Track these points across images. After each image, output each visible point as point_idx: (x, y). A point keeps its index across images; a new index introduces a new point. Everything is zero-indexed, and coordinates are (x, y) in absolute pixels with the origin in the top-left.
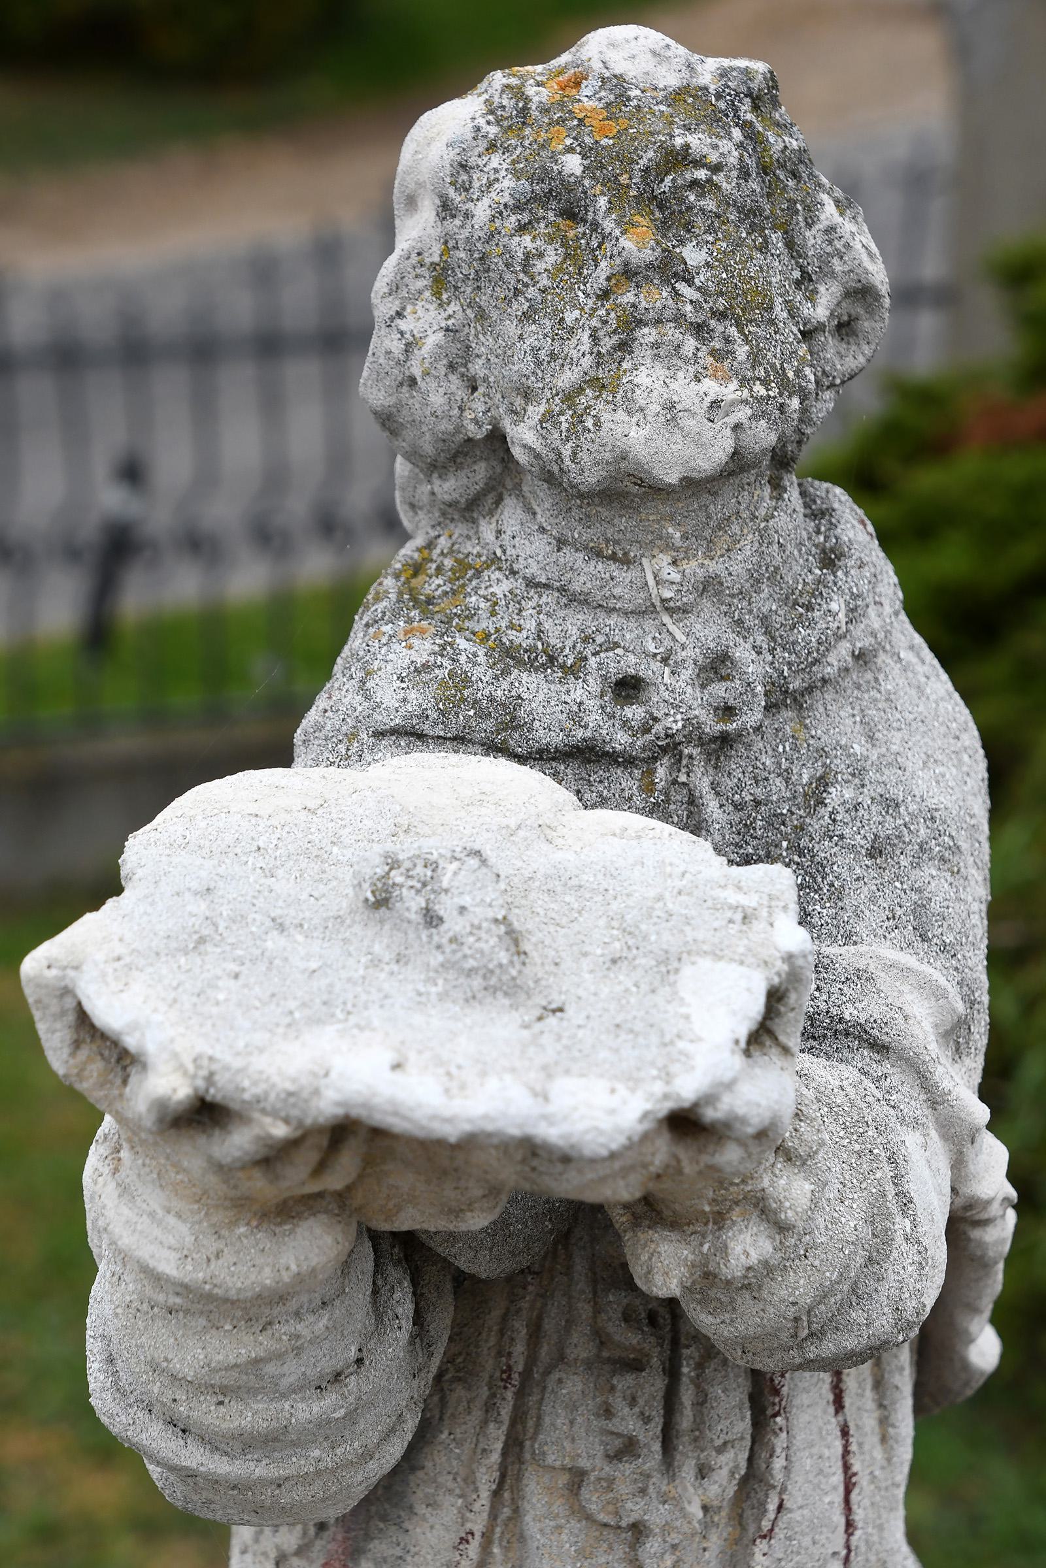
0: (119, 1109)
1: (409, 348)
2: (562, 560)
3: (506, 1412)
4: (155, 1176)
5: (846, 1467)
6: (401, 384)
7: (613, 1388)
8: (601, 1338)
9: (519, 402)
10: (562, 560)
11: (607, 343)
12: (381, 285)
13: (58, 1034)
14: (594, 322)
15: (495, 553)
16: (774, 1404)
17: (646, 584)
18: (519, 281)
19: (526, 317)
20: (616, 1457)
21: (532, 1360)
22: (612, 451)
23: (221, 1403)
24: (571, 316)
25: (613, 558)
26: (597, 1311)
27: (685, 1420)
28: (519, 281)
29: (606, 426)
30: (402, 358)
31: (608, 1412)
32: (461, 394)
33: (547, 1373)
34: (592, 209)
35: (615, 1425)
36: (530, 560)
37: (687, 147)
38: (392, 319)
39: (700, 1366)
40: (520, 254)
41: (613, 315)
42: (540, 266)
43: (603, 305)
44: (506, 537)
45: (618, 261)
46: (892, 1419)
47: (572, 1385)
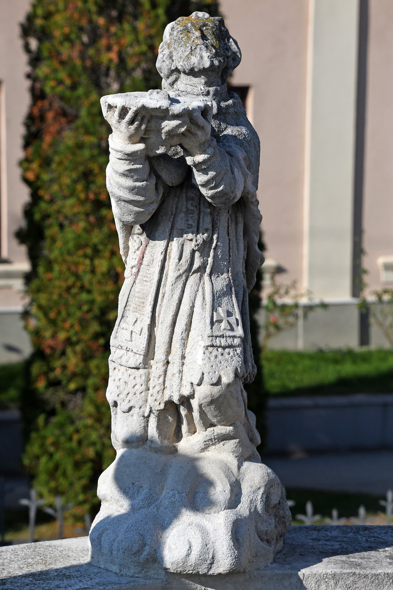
3: (171, 220)
5: (229, 245)
12: (160, 47)
21: (176, 212)
24: (188, 45)
26: (187, 204)
31: (188, 220)
32: (171, 62)
35: (189, 223)
39: (203, 216)
42: (184, 39)
46: (239, 245)
47: (182, 215)
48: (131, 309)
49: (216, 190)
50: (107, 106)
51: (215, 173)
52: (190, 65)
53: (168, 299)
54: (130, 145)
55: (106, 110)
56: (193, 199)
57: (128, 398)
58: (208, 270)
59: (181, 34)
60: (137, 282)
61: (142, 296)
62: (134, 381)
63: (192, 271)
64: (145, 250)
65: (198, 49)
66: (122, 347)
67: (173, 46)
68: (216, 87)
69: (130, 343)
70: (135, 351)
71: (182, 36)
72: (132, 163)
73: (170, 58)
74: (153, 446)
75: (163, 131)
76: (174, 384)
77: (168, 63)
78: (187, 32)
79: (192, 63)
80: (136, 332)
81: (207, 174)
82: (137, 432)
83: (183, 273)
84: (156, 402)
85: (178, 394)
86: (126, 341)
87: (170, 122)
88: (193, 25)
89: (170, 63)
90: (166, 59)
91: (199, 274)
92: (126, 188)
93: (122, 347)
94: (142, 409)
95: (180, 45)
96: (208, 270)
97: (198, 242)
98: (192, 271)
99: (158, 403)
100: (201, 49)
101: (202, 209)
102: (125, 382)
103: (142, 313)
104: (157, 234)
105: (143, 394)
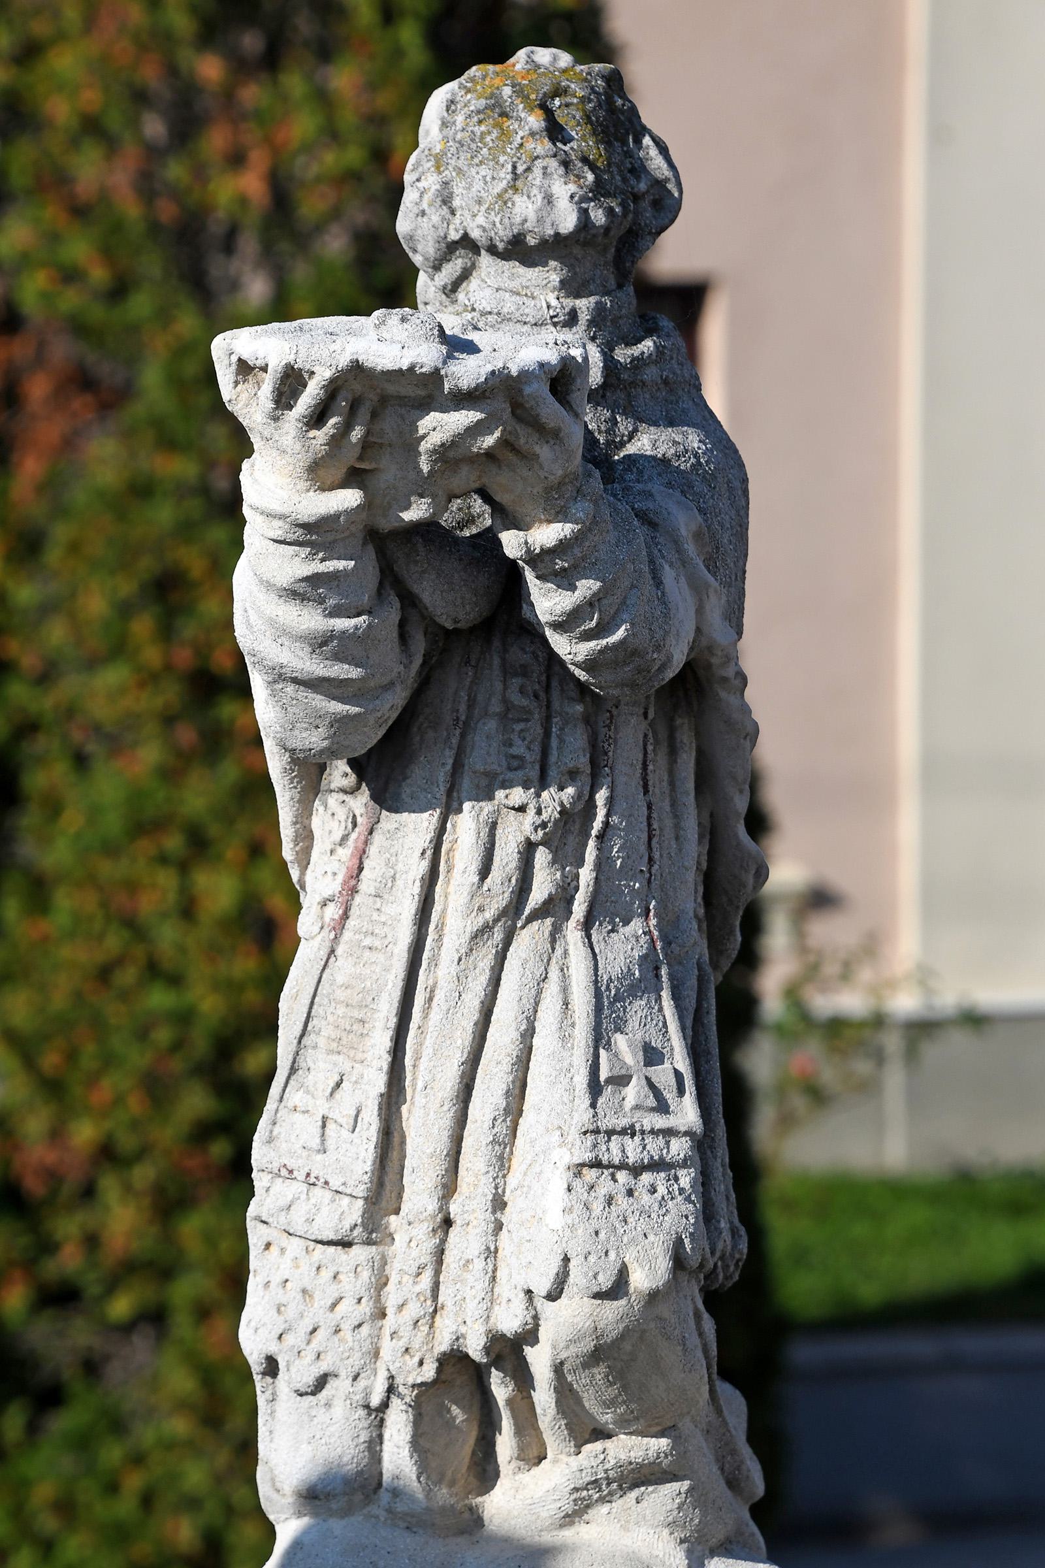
24: (502, 159)
31: (509, 744)
32: (449, 216)
35: (514, 751)
42: (488, 139)
47: (491, 725)
48: (322, 1042)
49: (604, 642)
52: (512, 225)
53: (444, 1008)
54: (311, 493)
57: (316, 1344)
58: (579, 908)
59: (480, 122)
60: (340, 951)
61: (356, 999)
62: (334, 1287)
63: (527, 912)
64: (366, 843)
66: (291, 1172)
69: (320, 1157)
70: (335, 1183)
71: (483, 128)
72: (321, 555)
74: (400, 1507)
76: (469, 1294)
77: (435, 219)
79: (518, 220)
80: (340, 1120)
81: (573, 588)
82: (345, 1459)
83: (496, 920)
84: (407, 1357)
85: (482, 1329)
86: (305, 1153)
87: (445, 416)
88: (519, 91)
89: (443, 219)
90: (430, 205)
91: (549, 921)
92: (301, 638)
93: (291, 1172)
94: (362, 1383)
96: (579, 908)
97: (545, 816)
98: (527, 912)
99: (416, 1359)
102: (304, 1291)
103: (360, 1056)
104: (406, 791)
105: (365, 1330)
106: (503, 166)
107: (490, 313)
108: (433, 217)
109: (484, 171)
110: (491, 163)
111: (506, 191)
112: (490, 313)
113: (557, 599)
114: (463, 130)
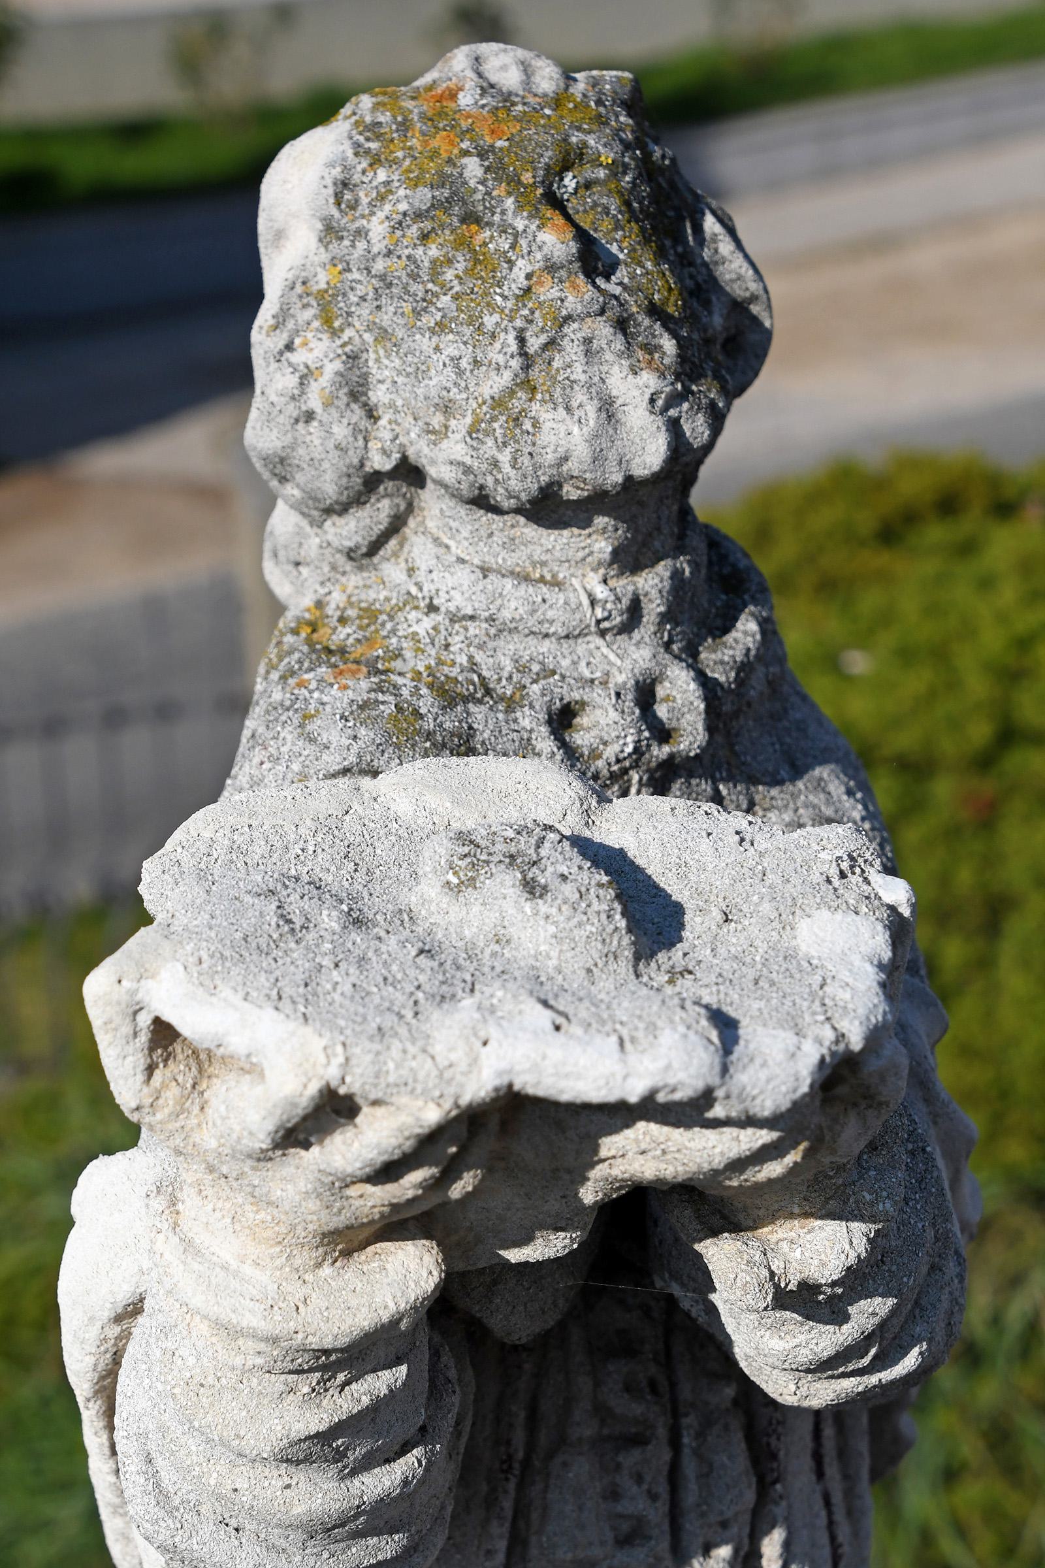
0: (198, 1140)
1: (303, 381)
2: (490, 587)
3: (508, 1504)
4: (229, 1220)
5: (833, 1538)
6: (297, 421)
7: (618, 1466)
8: (602, 1412)
9: (437, 420)
10: (490, 587)
11: (534, 344)
13: (130, 1059)
14: (519, 323)
15: (409, 593)
16: (772, 1470)
17: (581, 604)
18: (427, 292)
19: (441, 327)
20: (625, 1541)
21: (530, 1447)
22: (555, 451)
23: (288, 1486)
24: (490, 321)
25: (542, 580)
26: (597, 1384)
27: (691, 1495)
28: (427, 292)
29: (546, 427)
30: (296, 392)
31: (614, 1494)
32: (365, 423)
33: (550, 1456)
34: (498, 210)
35: (625, 1507)
36: (452, 592)
37: (585, 144)
38: (281, 353)
39: (701, 1435)
40: (427, 264)
41: (537, 314)
42: (449, 275)
43: (525, 306)
44: (421, 576)
45: (539, 256)
49: (874, 1379)
50: (144, 1038)
51: (891, 1302)
52: (536, 467)
54: (327, 1271)
55: (142, 1062)
56: (626, 1348)
59: (425, 237)
65: (572, 350)
67: (365, 311)
68: (669, 562)
71: (434, 251)
73: (354, 396)
75: (597, 1173)
77: (340, 432)
78: (463, 221)
79: (550, 458)
88: (497, 169)
89: (356, 431)
90: (327, 405)
95: (428, 320)
100: (590, 351)
101: (686, 1392)
106: (493, 336)
107: (472, 618)
108: (335, 429)
109: (451, 347)
110: (467, 331)
111: (512, 393)
112: (472, 618)
113: (802, 1338)
114: (389, 253)
